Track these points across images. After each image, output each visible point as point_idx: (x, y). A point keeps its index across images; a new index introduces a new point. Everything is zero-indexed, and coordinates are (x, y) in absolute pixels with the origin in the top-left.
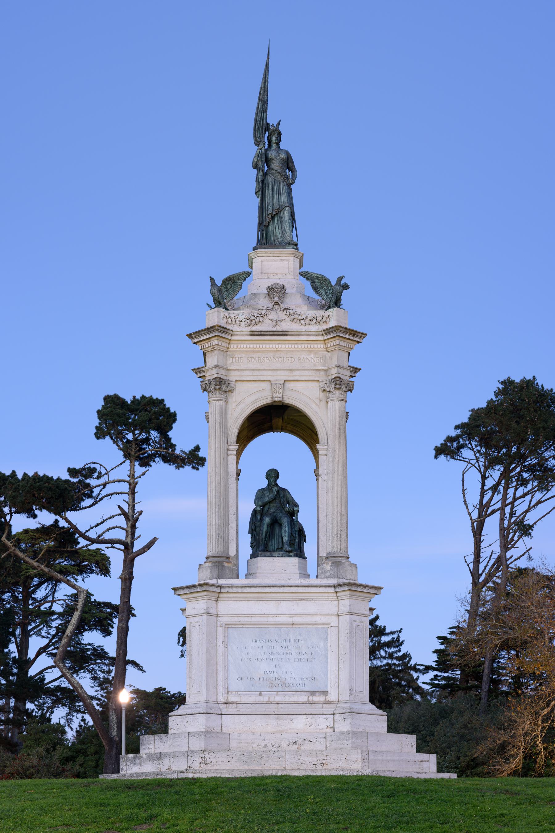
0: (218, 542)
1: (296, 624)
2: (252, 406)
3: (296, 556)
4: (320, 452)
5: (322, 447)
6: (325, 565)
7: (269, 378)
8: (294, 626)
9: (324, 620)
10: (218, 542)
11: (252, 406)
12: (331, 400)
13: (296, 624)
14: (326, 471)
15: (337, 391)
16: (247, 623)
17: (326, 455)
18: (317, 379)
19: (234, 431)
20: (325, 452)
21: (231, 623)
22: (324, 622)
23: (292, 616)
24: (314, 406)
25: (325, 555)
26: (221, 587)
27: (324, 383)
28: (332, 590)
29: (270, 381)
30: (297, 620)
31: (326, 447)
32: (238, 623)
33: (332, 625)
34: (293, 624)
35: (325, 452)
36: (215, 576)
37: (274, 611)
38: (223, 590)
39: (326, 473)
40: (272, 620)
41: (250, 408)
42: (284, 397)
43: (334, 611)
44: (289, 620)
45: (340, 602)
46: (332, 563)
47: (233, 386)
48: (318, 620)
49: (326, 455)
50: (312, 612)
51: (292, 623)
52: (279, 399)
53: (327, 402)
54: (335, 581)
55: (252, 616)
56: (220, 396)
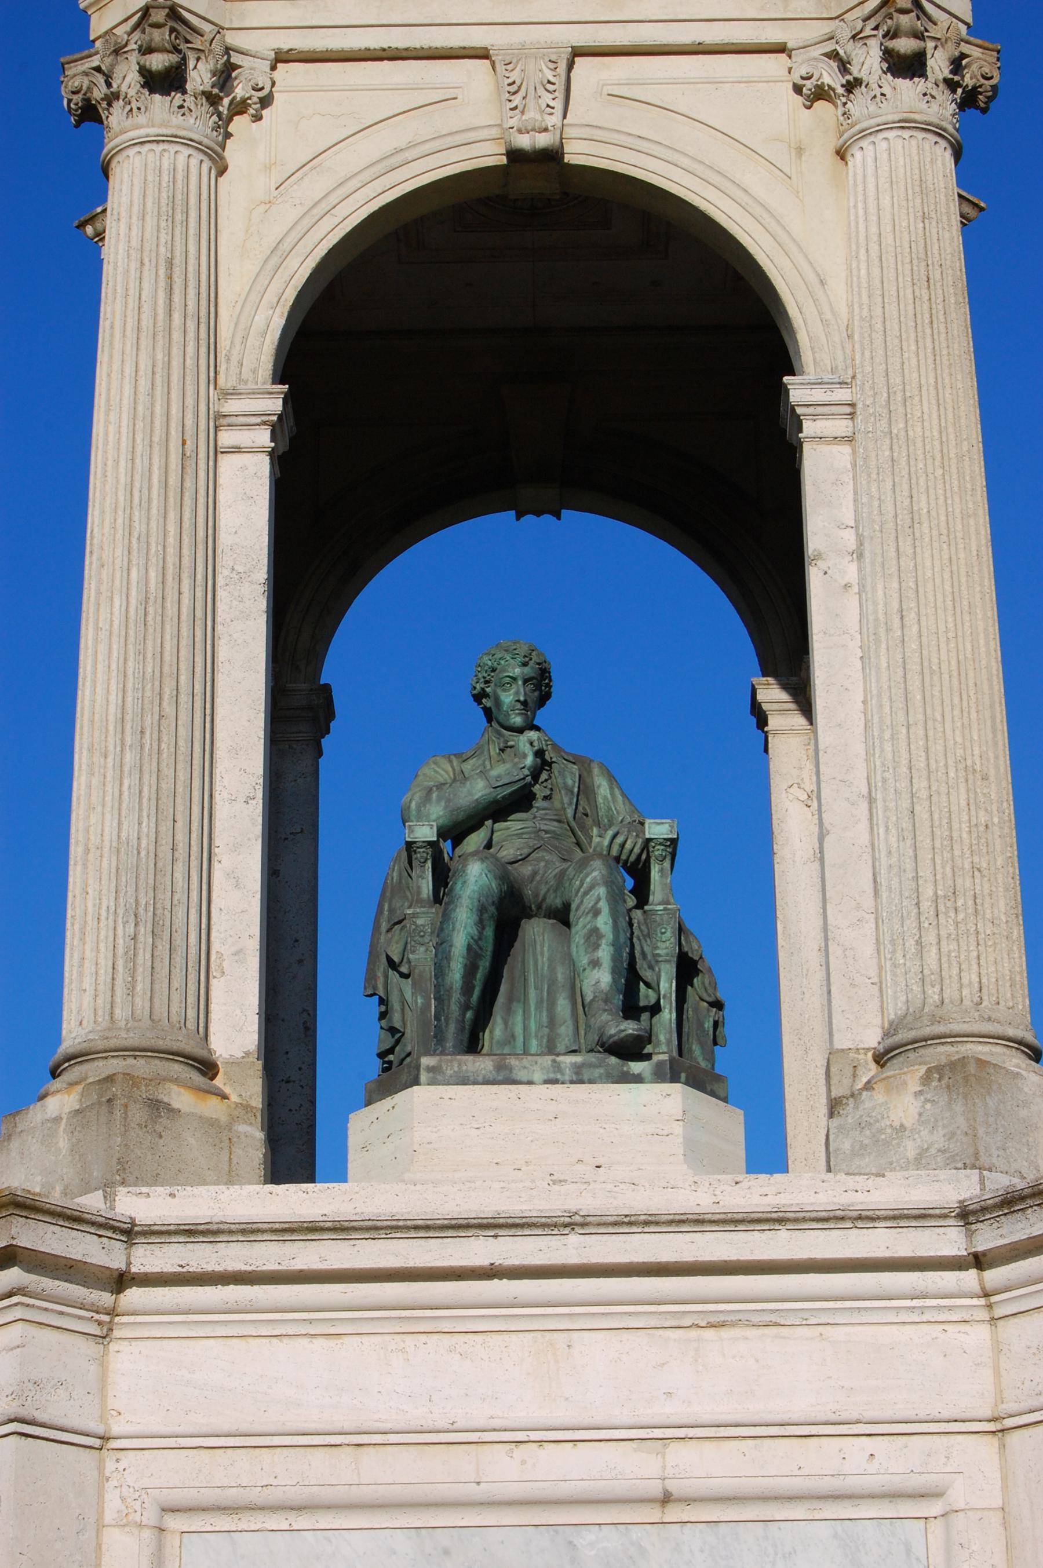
0: (132, 958)
1: (689, 1501)
2: (378, 186)
3: (671, 1073)
4: (809, 428)
5: (818, 395)
6: (879, 1096)
7: (476, 38)
8: (673, 1513)
9: (893, 1462)
10: (132, 958)
11: (378, 186)
12: (864, 134)
13: (689, 1501)
14: (849, 538)
15: (903, 84)
16: (328, 1494)
17: (850, 440)
18: (772, 34)
19: (260, 319)
20: (841, 427)
21: (210, 1496)
22: (897, 1483)
23: (658, 1435)
24: (753, 177)
25: (872, 1038)
26: (130, 1233)
27: (817, 51)
28: (950, 1241)
29: (482, 54)
30: (696, 1466)
31: (842, 395)
32: (255, 1496)
33: (958, 1496)
34: (666, 1499)
35: (841, 427)
36: (97, 1174)
37: (525, 1408)
38: (147, 1259)
39: (851, 543)
40: (505, 1470)
41: (361, 196)
42: (569, 132)
43: (973, 1396)
44: (636, 1468)
45: (1009, 1330)
46: (926, 1079)
47: (263, 81)
48: (855, 1462)
49: (850, 440)
50: (801, 1404)
51: (655, 1489)
52: (543, 141)
53: (841, 154)
54: (961, 1188)
55: (361, 1439)
56: (177, 119)
